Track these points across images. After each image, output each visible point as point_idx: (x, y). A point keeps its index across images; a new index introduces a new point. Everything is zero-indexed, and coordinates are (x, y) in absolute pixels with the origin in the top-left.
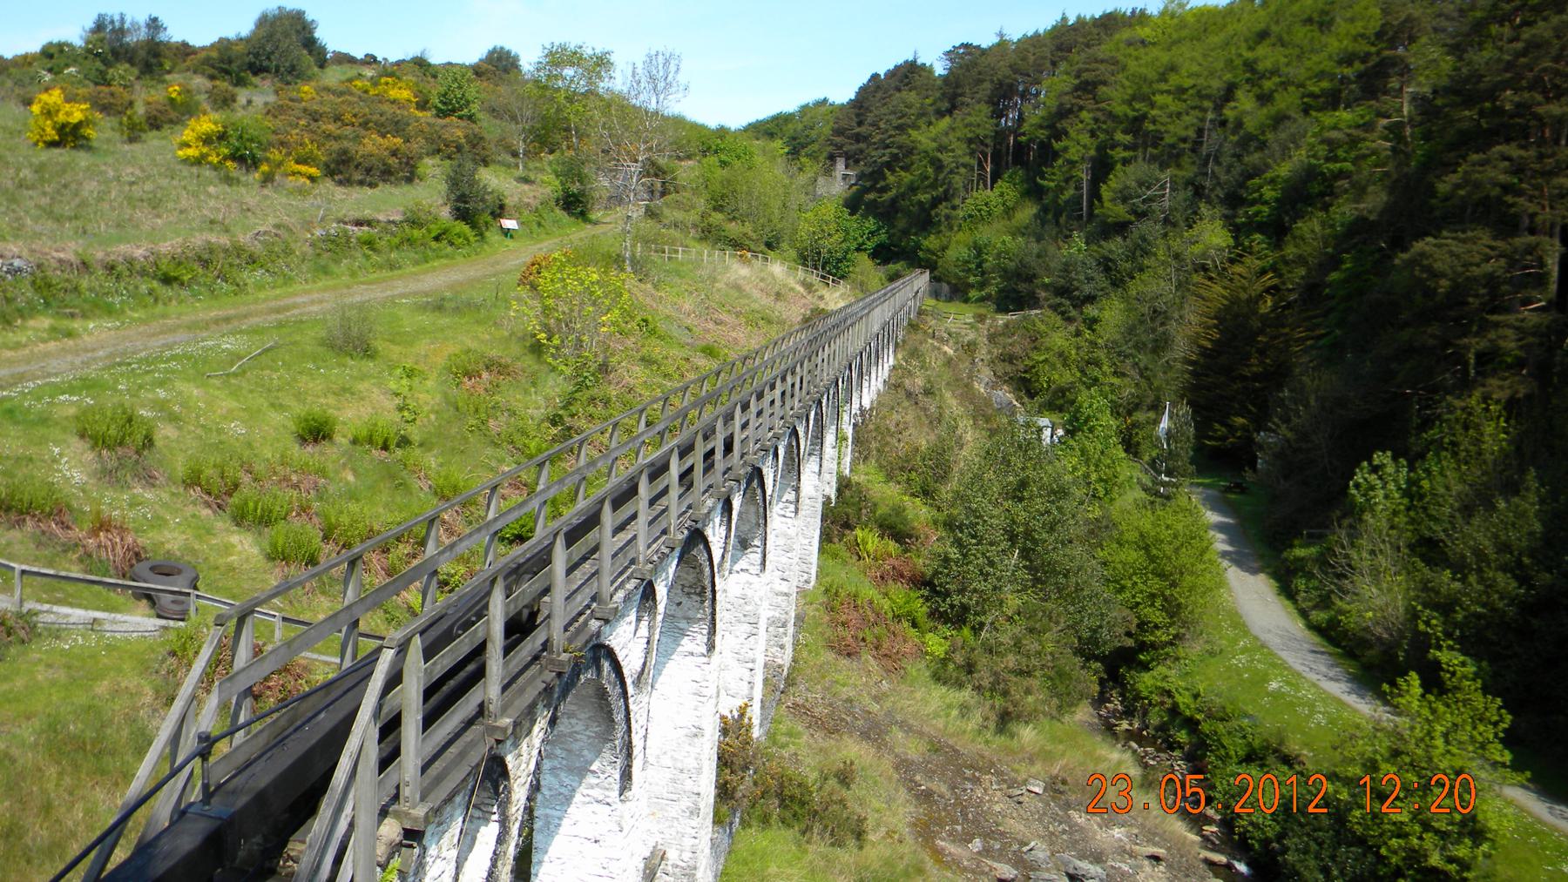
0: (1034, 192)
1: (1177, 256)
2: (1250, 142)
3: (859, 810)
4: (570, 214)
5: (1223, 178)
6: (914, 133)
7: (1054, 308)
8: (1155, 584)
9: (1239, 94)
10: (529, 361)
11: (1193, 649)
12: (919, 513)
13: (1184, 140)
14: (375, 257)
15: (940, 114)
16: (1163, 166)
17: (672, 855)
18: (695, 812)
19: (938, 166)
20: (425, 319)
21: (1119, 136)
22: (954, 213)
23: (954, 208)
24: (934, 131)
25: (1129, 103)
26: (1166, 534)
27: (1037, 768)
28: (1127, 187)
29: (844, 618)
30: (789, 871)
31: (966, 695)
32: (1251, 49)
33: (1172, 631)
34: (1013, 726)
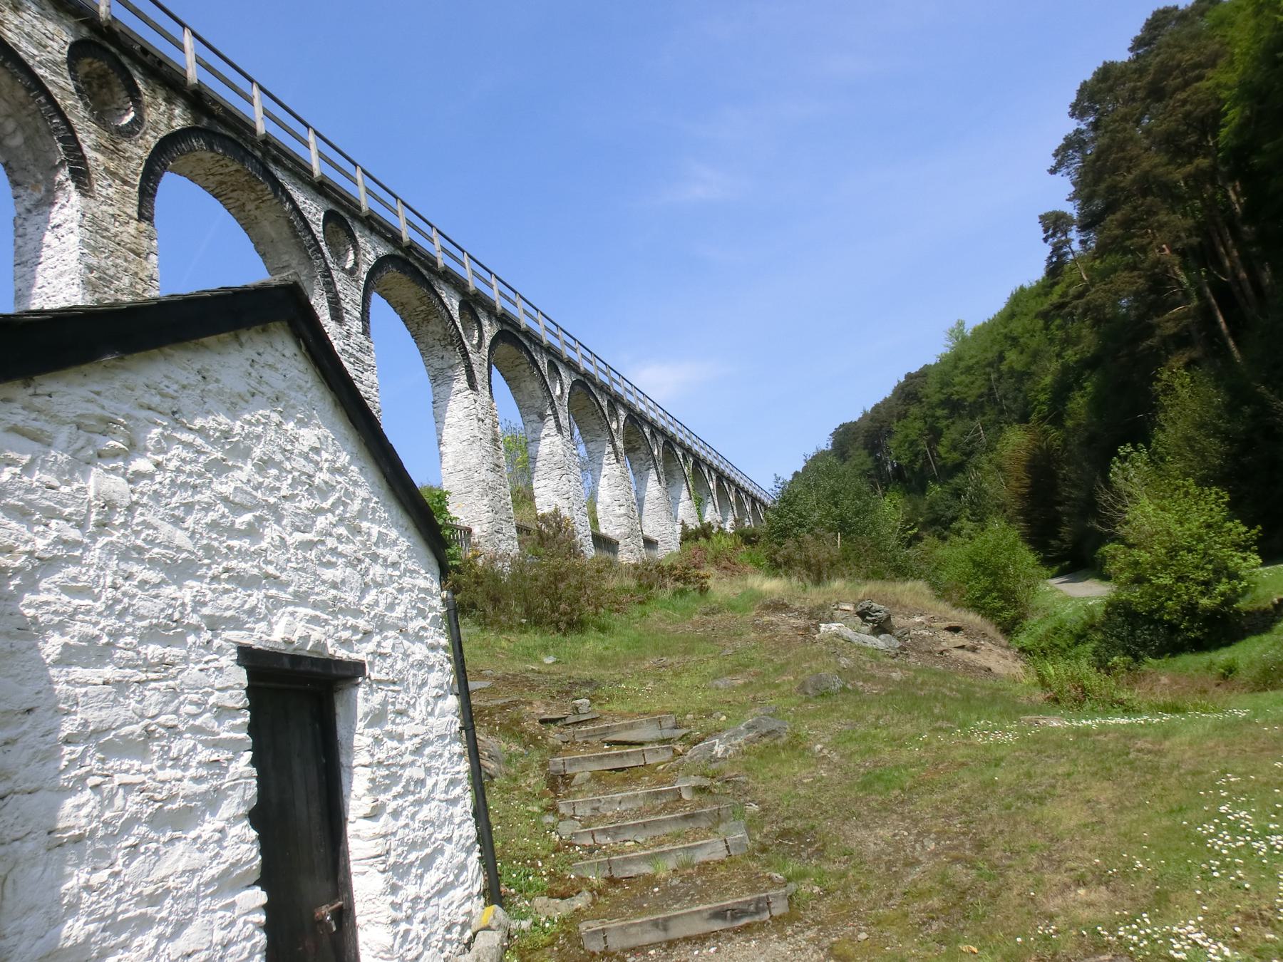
2: (1022, 376)
5: (1013, 407)
9: (1007, 354)
13: (981, 396)
16: (973, 418)
21: (939, 412)
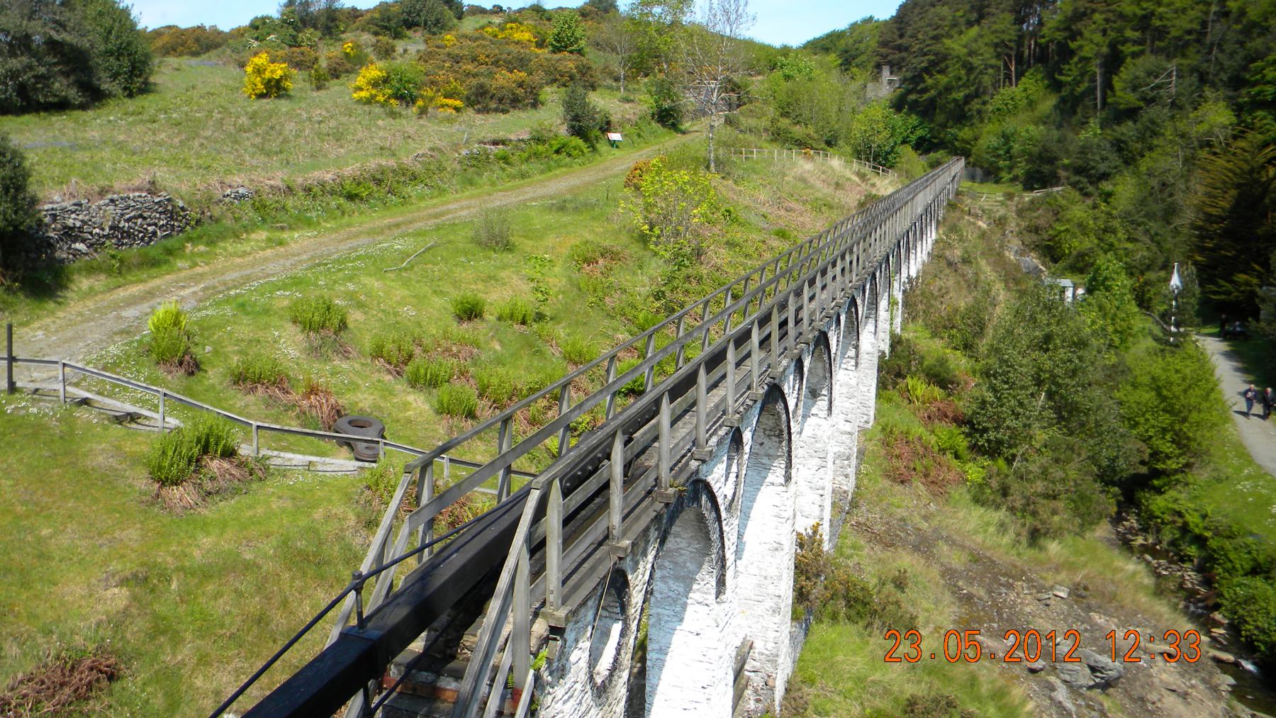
0: (1056, 86)
1: (1183, 136)
3: (911, 609)
4: (664, 126)
6: (947, 42)
7: (1074, 185)
8: (1166, 419)
10: (635, 248)
11: (1200, 476)
12: (959, 363)
14: (509, 169)
15: (970, 24)
16: (1169, 57)
17: (759, 645)
18: (777, 611)
19: (970, 69)
20: (550, 218)
21: (1129, 33)
22: (984, 108)
23: (984, 103)
24: (964, 39)
26: (1175, 378)
27: (1063, 576)
28: (1137, 78)
29: (897, 452)
30: (853, 659)
31: (1002, 514)
33: (1182, 460)
34: (1042, 541)
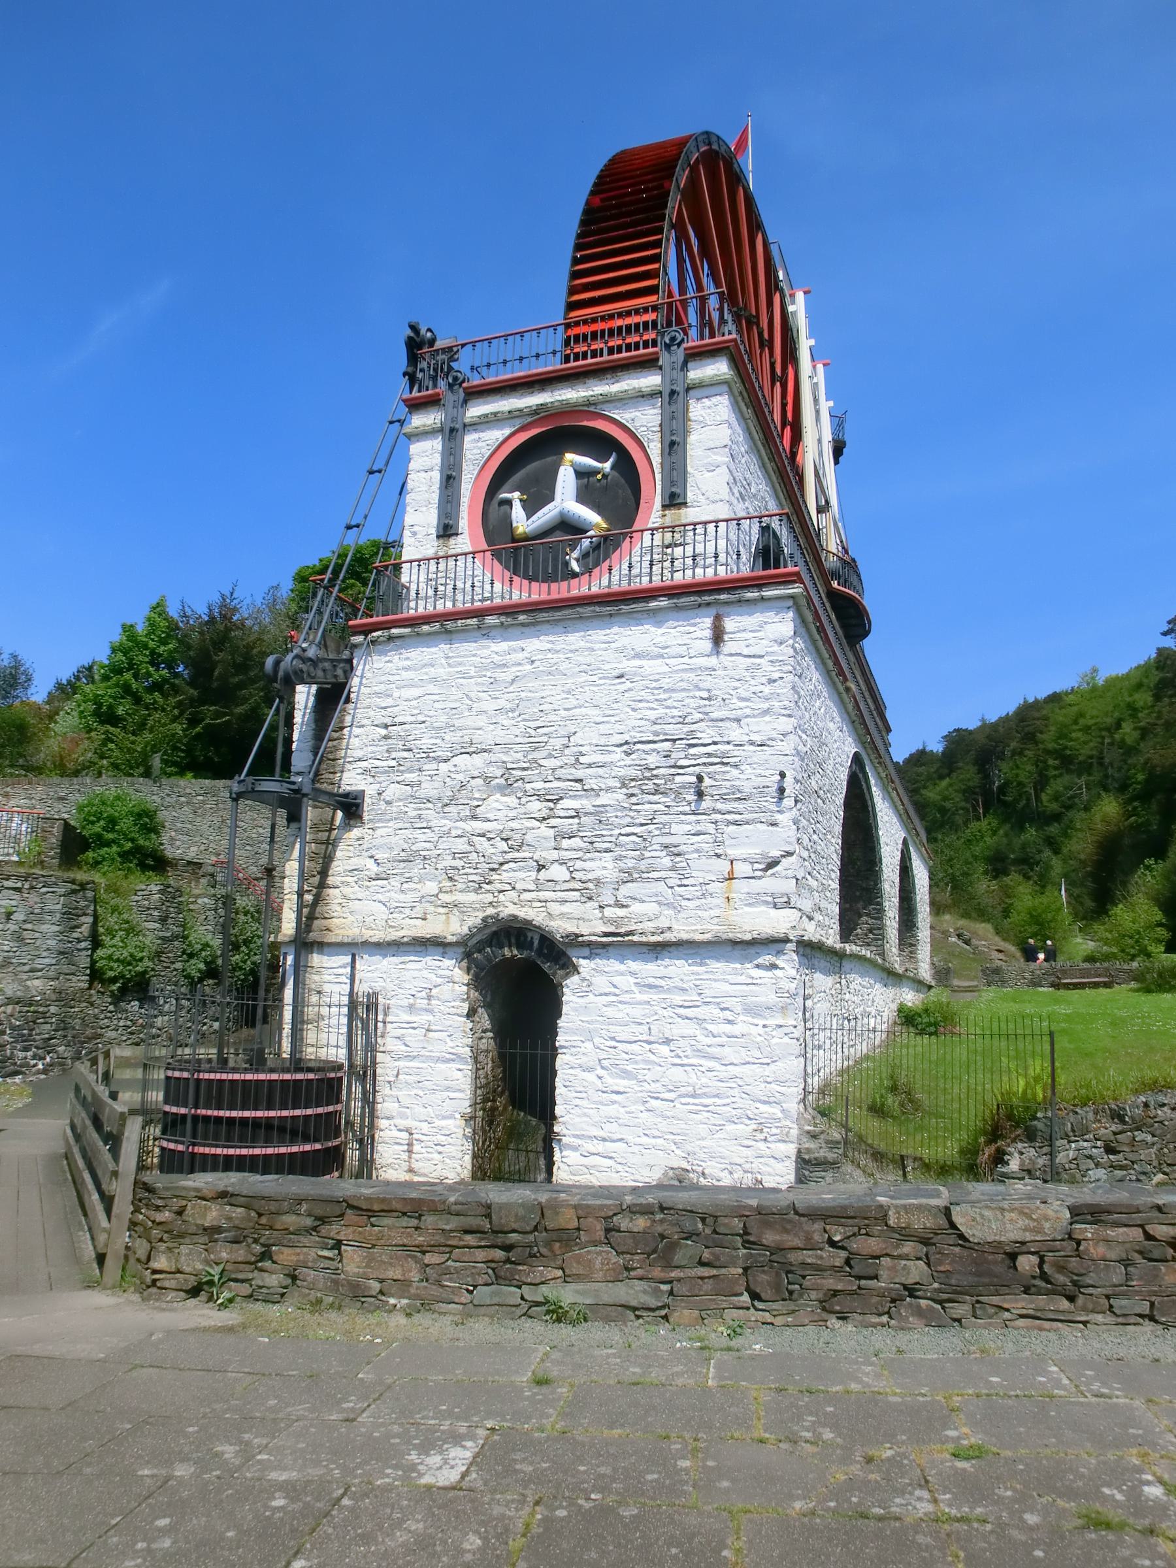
2: (1130, 751)
6: (923, 792)
7: (1020, 872)
8: (1035, 928)
9: (1124, 725)
13: (1091, 757)
15: (941, 777)
25: (1055, 741)
32: (1131, 695)
